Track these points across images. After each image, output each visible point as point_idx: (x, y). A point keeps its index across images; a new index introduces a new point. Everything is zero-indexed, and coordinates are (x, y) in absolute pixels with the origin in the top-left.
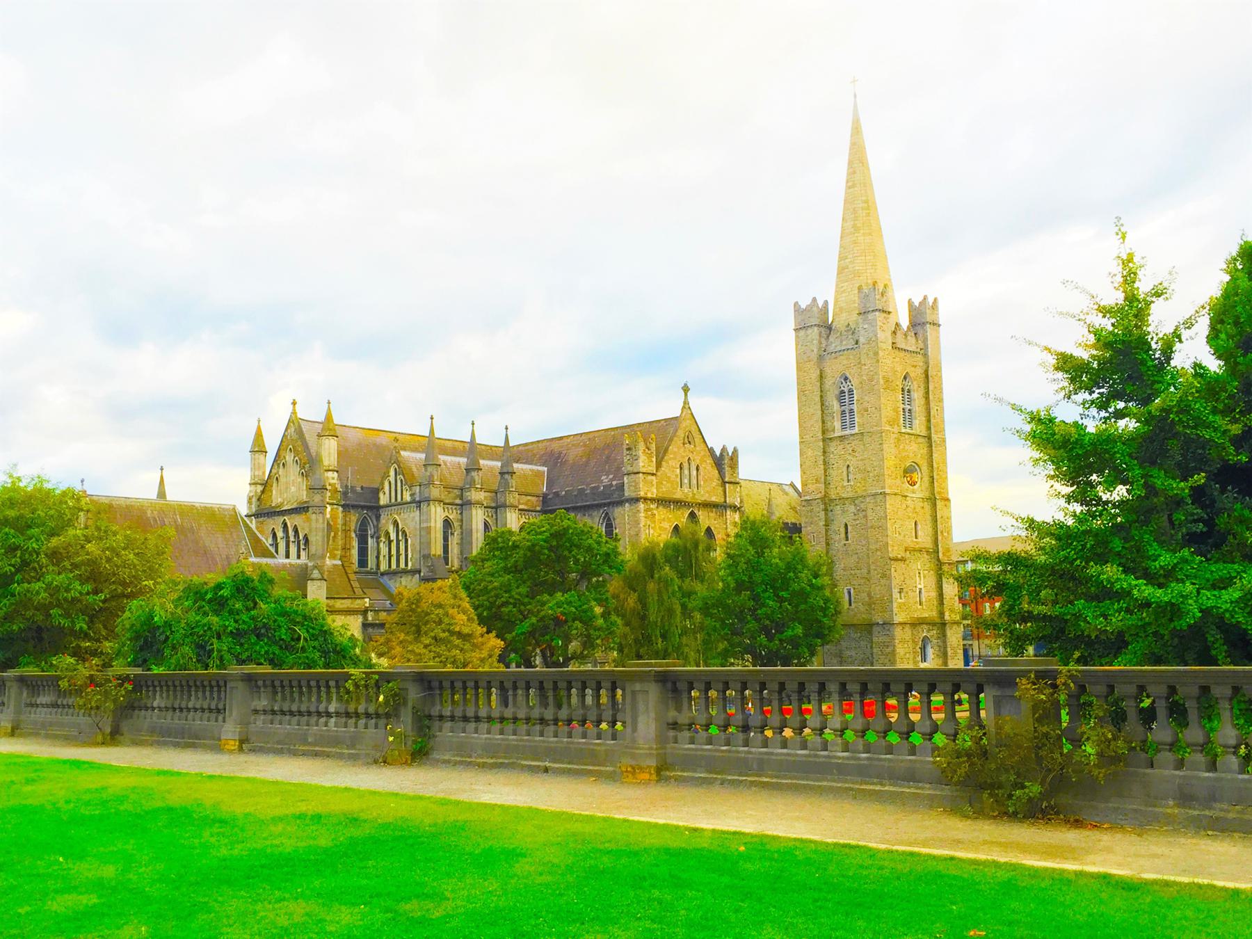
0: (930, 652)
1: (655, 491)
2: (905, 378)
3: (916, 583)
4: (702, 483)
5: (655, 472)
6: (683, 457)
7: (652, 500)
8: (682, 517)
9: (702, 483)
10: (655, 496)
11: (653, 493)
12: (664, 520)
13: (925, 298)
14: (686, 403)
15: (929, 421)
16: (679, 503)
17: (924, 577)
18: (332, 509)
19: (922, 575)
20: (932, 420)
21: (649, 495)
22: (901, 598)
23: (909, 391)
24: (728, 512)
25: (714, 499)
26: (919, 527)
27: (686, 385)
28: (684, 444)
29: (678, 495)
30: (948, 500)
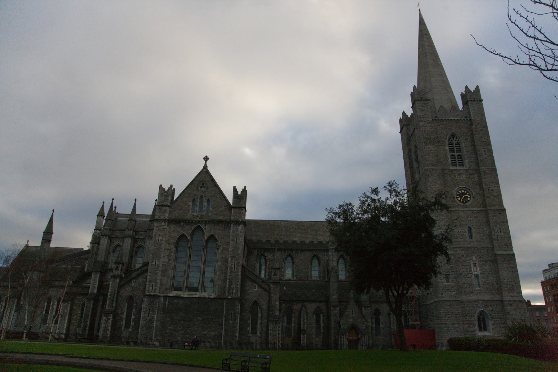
0: (490, 324)
1: (167, 215)
2: (453, 136)
3: (471, 271)
4: (211, 209)
5: (169, 204)
6: (196, 195)
7: (164, 220)
8: (187, 231)
9: (211, 209)
10: (167, 218)
11: (167, 216)
12: (174, 231)
13: (466, 87)
14: (205, 167)
15: (477, 159)
16: (188, 222)
17: (480, 266)
18: (93, 246)
19: (477, 265)
20: (480, 158)
21: (162, 218)
22: (448, 281)
23: (458, 144)
24: (232, 225)
25: (221, 218)
26: (473, 230)
27: (206, 156)
28: (197, 188)
29: (188, 217)
30: (504, 210)
